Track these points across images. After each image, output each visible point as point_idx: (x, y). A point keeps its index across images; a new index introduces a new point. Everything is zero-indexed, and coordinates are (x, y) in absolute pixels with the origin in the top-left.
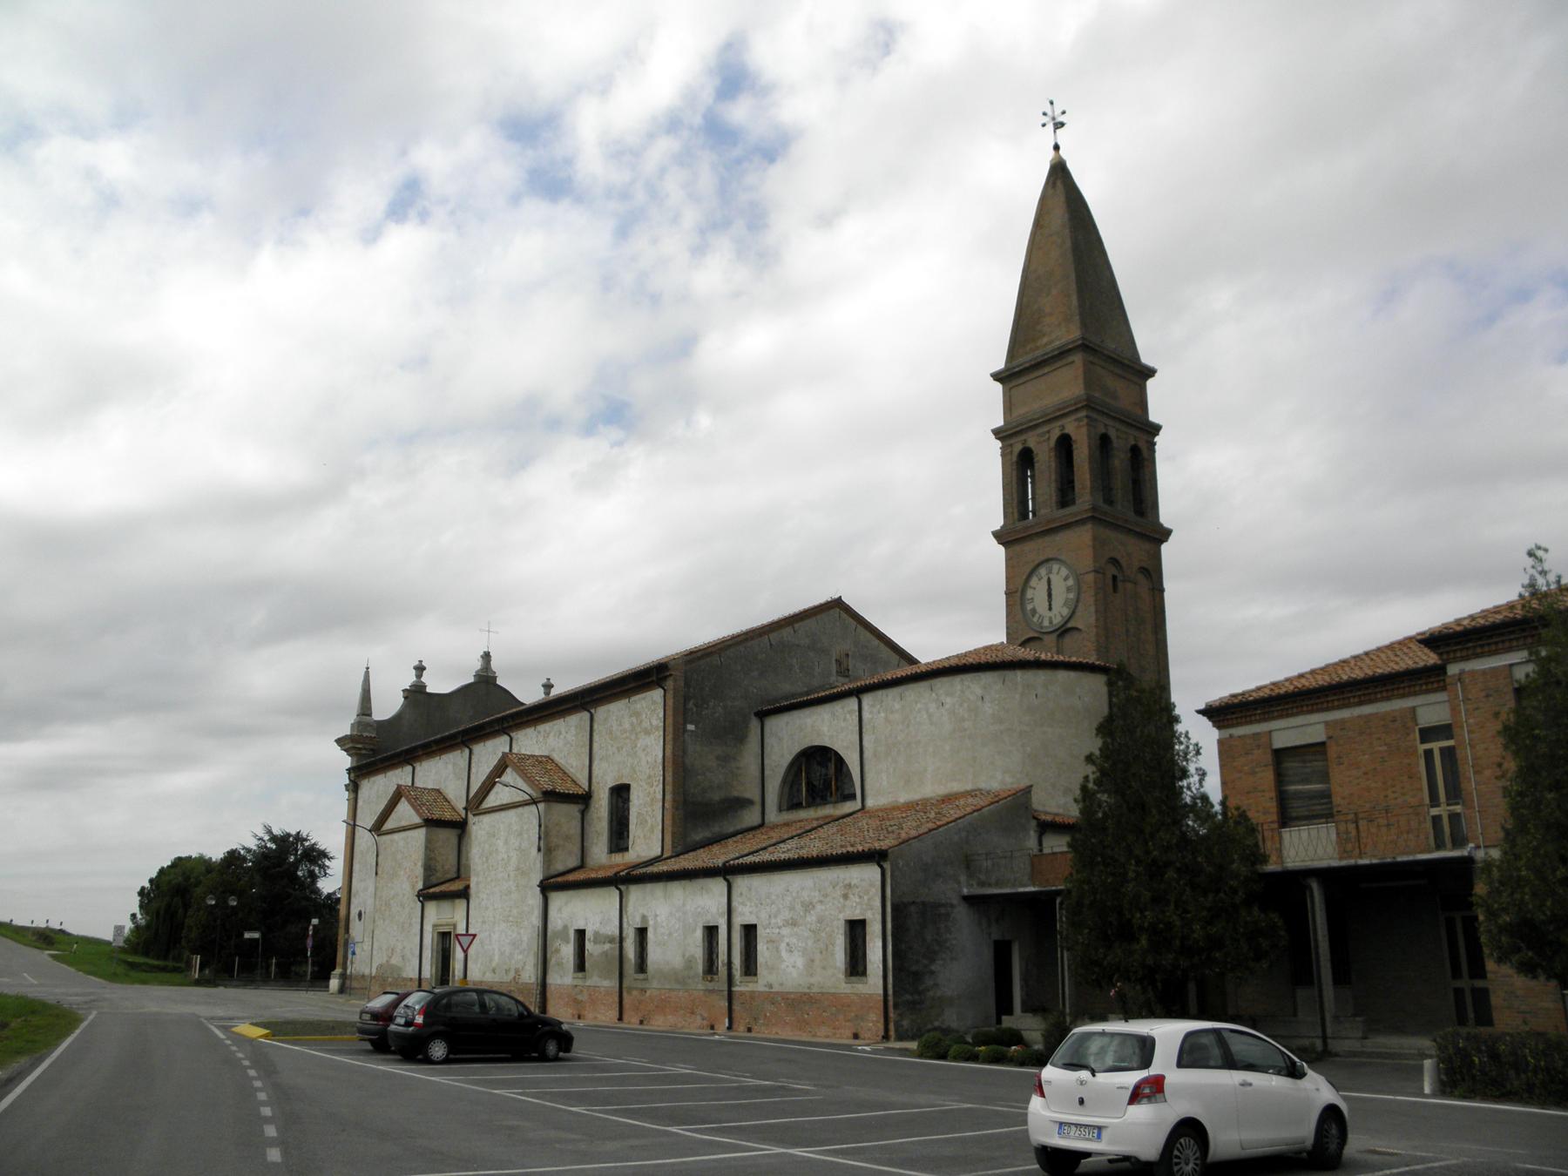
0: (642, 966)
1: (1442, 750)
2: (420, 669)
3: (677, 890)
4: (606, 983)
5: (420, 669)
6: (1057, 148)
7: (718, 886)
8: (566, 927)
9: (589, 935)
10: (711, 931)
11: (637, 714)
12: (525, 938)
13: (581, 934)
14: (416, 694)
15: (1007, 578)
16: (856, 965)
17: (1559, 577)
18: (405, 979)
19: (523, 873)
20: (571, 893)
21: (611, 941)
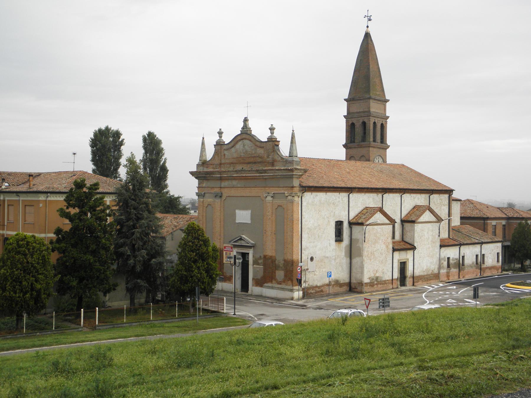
0: (463, 265)
1: (22, 200)
2: (220, 133)
3: (471, 247)
4: (455, 270)
5: (220, 133)
6: (368, 27)
7: (478, 246)
8: (445, 257)
9: (451, 258)
10: (477, 256)
11: (441, 199)
12: (435, 261)
13: (448, 258)
14: (219, 144)
15: (346, 155)
16: (498, 261)
17: (124, 139)
18: (385, 281)
19: (434, 242)
20: (446, 248)
21: (456, 259)
